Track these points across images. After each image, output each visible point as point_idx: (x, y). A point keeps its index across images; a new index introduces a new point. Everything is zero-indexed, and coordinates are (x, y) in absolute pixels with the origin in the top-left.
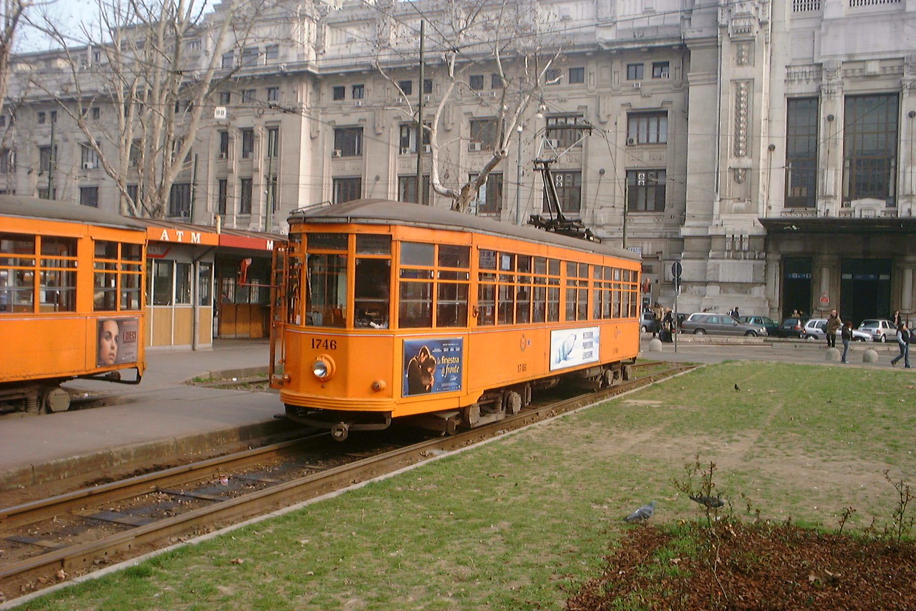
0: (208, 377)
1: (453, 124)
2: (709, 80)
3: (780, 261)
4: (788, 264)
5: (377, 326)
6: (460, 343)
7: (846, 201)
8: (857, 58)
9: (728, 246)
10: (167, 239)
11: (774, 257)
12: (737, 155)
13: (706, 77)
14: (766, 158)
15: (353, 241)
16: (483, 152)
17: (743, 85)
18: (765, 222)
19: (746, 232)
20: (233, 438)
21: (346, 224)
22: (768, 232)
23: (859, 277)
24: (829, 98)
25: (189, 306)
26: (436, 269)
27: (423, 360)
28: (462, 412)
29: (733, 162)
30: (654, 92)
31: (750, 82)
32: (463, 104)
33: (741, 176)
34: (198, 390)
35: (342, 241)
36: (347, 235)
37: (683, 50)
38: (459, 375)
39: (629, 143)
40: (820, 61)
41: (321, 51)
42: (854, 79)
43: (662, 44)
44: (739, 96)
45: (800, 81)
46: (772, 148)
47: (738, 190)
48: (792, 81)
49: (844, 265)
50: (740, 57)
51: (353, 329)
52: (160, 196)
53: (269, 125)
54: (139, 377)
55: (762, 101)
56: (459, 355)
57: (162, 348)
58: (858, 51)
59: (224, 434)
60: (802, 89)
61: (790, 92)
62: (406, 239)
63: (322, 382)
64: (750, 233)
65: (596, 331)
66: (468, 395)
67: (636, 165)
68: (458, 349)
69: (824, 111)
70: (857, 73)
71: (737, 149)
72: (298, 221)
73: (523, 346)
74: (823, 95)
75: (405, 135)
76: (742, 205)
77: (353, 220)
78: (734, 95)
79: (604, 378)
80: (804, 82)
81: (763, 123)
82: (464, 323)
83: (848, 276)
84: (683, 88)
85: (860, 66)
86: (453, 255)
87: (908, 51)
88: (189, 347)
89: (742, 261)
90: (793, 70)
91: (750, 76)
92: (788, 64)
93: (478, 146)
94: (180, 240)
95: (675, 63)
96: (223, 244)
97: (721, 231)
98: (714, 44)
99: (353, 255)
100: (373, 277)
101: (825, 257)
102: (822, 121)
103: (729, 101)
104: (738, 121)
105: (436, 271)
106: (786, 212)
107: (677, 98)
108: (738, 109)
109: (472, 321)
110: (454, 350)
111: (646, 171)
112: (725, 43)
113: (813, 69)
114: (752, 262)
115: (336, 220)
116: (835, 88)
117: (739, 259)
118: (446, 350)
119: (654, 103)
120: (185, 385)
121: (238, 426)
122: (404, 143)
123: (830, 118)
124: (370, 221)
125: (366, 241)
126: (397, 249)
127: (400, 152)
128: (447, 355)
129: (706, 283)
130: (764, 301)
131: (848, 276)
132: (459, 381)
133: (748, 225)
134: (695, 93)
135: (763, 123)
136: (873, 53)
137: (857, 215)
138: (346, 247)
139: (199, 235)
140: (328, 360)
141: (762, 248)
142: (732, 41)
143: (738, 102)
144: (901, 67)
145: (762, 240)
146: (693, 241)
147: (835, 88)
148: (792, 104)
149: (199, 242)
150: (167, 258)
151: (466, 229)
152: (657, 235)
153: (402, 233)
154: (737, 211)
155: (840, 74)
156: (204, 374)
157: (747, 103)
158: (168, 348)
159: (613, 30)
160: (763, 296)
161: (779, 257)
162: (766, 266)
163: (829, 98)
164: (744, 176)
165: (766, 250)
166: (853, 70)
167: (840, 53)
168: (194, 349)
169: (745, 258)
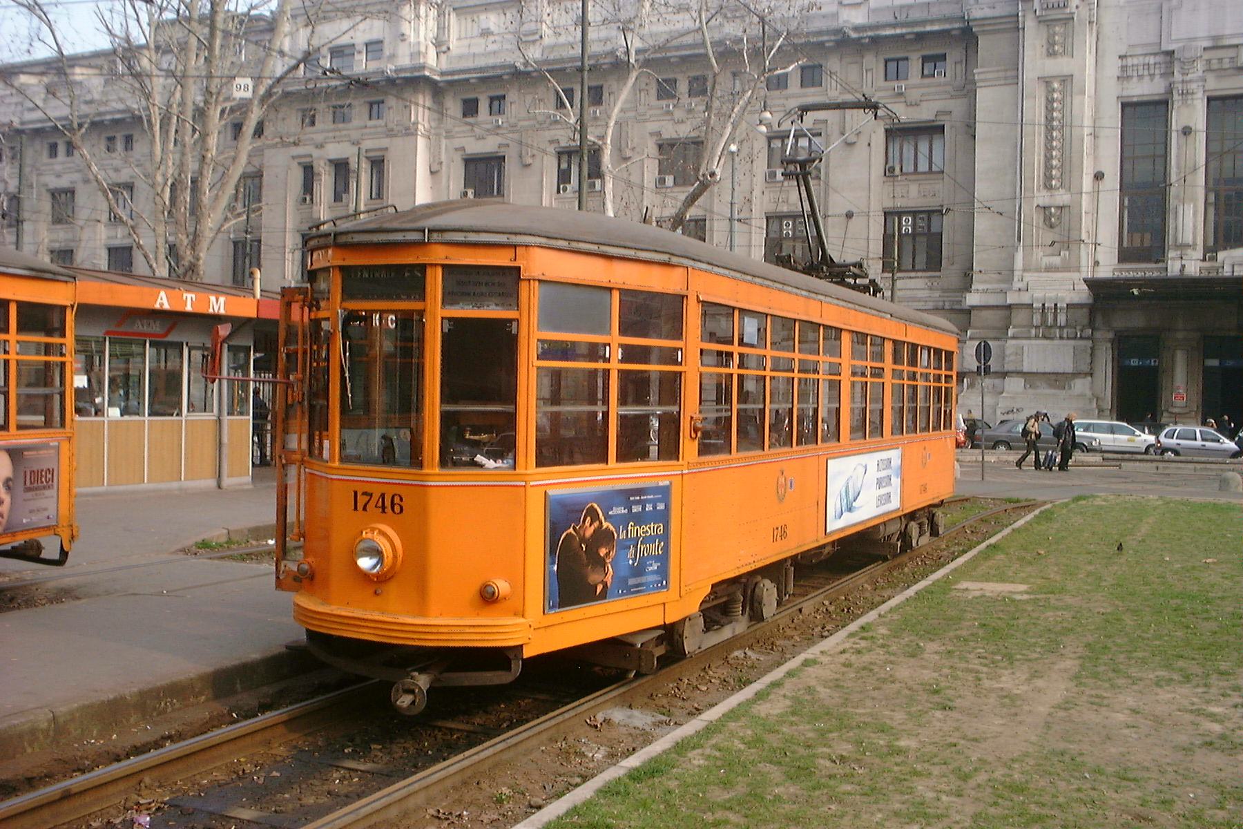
0: (223, 539)
1: (633, 149)
2: (1006, 78)
3: (1112, 342)
4: (1123, 345)
5: (490, 464)
6: (665, 492)
7: (1210, 252)
8: (1227, 42)
9: (1037, 319)
10: (166, 306)
11: (1105, 335)
12: (1048, 187)
13: (1002, 74)
14: (1090, 189)
15: (435, 282)
16: (676, 189)
17: (1056, 85)
18: (1092, 284)
19: (1062, 300)
20: (200, 693)
21: (421, 244)
22: (1095, 300)
23: (1230, 363)
24: (1184, 102)
25: (210, 417)
26: (615, 341)
27: (590, 531)
28: (670, 634)
29: (1042, 198)
30: (920, 98)
31: (1066, 80)
32: (645, 121)
33: (1053, 217)
34: (203, 566)
35: (409, 280)
36: (423, 268)
37: (967, 37)
38: (664, 559)
39: (889, 172)
40: (1170, 48)
41: (444, 48)
42: (1220, 72)
43: (936, 28)
44: (1050, 101)
45: (1140, 77)
46: (1099, 176)
47: (1049, 236)
48: (1129, 78)
49: (1209, 345)
50: (1051, 43)
51: (437, 470)
52: (193, 249)
53: (371, 154)
54: (64, 554)
55: (1084, 109)
56: (664, 517)
57: (163, 486)
58: (1227, 32)
59: (177, 691)
61: (1125, 94)
62: (551, 275)
63: (376, 582)
64: (1068, 301)
65: (895, 455)
66: (681, 601)
67: (900, 203)
68: (661, 507)
69: (1177, 120)
70: (1226, 64)
71: (1048, 178)
72: (322, 241)
73: (781, 491)
74: (1176, 97)
75: (564, 166)
76: (1056, 260)
77: (435, 235)
78: (1043, 99)
79: (905, 536)
80: (1147, 79)
81: (1087, 141)
82: (670, 450)
83: (1214, 363)
84: (968, 91)
85: (1231, 53)
86: (649, 313)
88: (212, 483)
89: (1056, 342)
90: (1130, 61)
91: (1066, 71)
92: (1123, 53)
93: (669, 180)
94: (189, 308)
95: (954, 55)
96: (263, 315)
97: (1025, 298)
98: (1013, 26)
99: (438, 313)
100: (483, 358)
101: (1180, 335)
102: (1174, 135)
103: (1035, 109)
104: (1049, 139)
105: (615, 346)
106: (1121, 271)
107: (957, 107)
108: (1049, 119)
109: (689, 447)
110: (650, 507)
111: (914, 213)
112: (1030, 24)
113: (1159, 59)
114: (1072, 342)
115: (398, 237)
116: (1194, 86)
117: (1052, 339)
118: (636, 509)
119: (925, 113)
120: (181, 556)
121: (210, 669)
122: (564, 177)
123: (1187, 131)
124: (473, 237)
125: (463, 281)
126: (532, 297)
127: (558, 192)
128: (640, 519)
130: (1090, 401)
131: (1214, 363)
132: (663, 572)
133: (1069, 289)
134: (985, 97)
135: (1087, 141)
137: (1227, 272)
138: (423, 297)
139: (222, 299)
140: (386, 537)
141: (1086, 321)
142: (1041, 21)
143: (1049, 110)
145: (1086, 311)
146: (985, 313)
147: (1194, 86)
149: (222, 311)
150: (172, 338)
151: (675, 260)
152: (930, 305)
153: (543, 264)
154: (1049, 269)
155: (1200, 66)
156: (217, 534)
157: (1062, 111)
158: (175, 485)
159: (864, 9)
160: (1089, 393)
161: (1111, 335)
162: (1092, 349)
163: (1184, 102)
164: (1059, 218)
165: (1091, 324)
167: (1201, 34)
168: (219, 487)
169: (1061, 338)
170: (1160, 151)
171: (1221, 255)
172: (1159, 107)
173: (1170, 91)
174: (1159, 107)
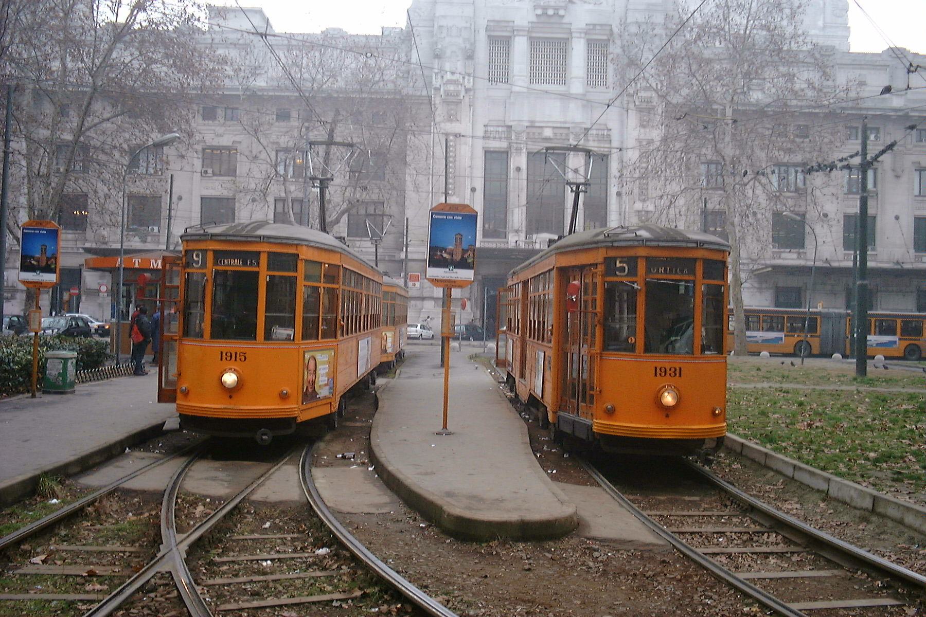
8: (537, 125)
40: (510, 124)
46: (473, 190)
58: (538, 119)
60: (495, 145)
61: (487, 145)
74: (513, 151)
85: (539, 130)
87: (573, 123)
90: (489, 129)
113: (505, 129)
129: (423, 299)
136: (548, 122)
142: (445, 102)
144: (567, 135)
148: (488, 155)
155: (524, 137)
157: (455, 152)
166: (534, 133)
170: (504, 177)
171: (535, 236)
172: (504, 155)
173: (510, 147)
174: (504, 155)
